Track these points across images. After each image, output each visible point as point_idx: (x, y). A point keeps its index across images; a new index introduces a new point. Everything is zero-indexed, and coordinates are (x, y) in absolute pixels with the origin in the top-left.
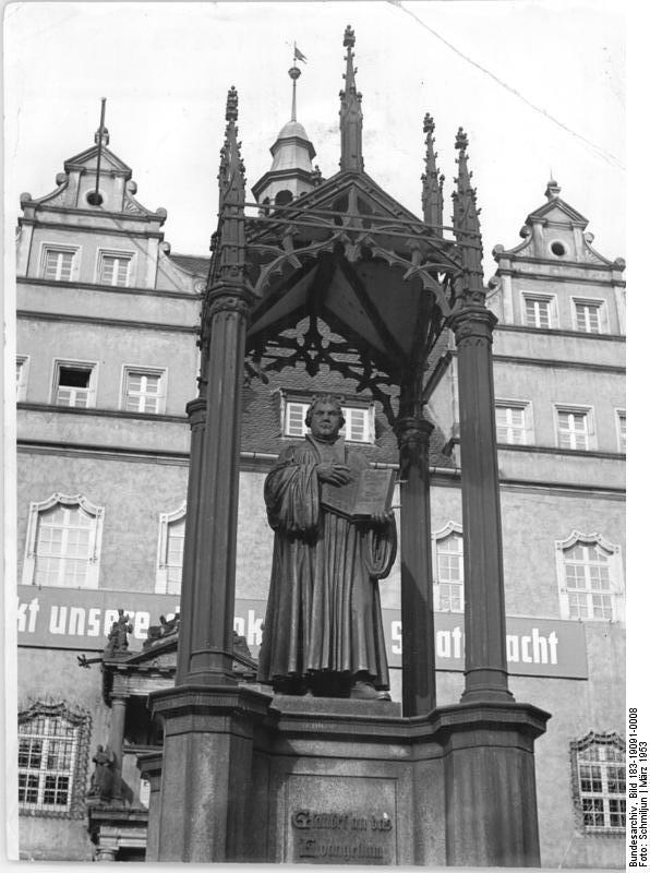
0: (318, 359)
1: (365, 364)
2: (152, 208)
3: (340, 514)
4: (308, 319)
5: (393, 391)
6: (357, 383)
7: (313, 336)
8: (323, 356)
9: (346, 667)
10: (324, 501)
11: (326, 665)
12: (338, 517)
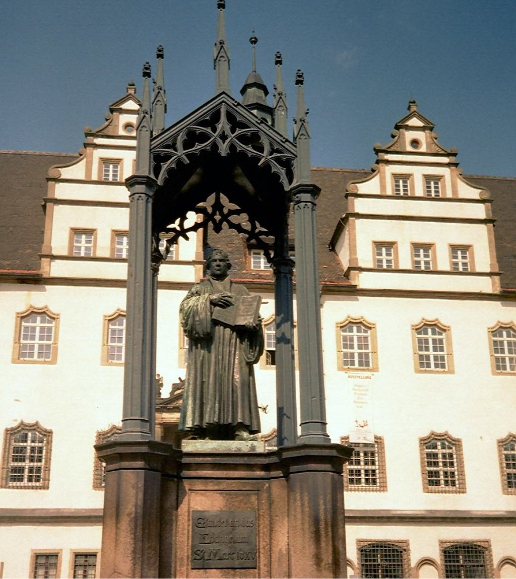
0: (221, 221)
1: (251, 221)
4: (214, 195)
6: (247, 236)
7: (218, 206)
8: (225, 218)
11: (216, 419)
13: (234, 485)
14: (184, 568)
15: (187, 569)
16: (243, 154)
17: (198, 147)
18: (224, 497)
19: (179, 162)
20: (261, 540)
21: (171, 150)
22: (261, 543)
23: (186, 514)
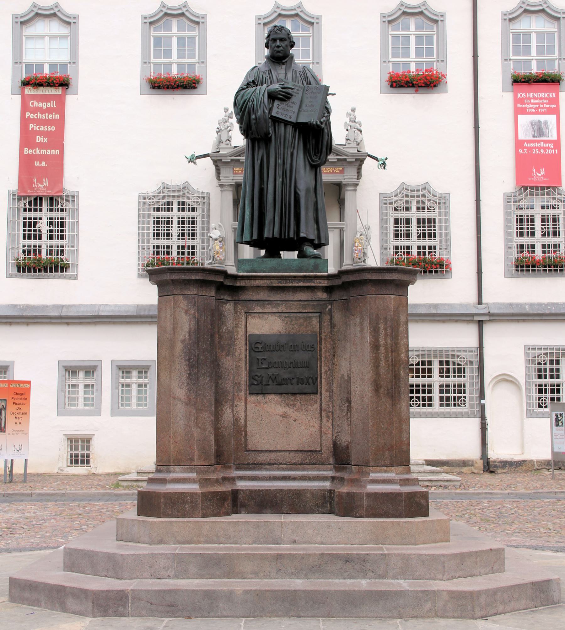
10: (274, 114)
11: (276, 235)
14: (242, 394)
15: (246, 394)
18: (283, 320)
20: (323, 365)
23: (243, 338)
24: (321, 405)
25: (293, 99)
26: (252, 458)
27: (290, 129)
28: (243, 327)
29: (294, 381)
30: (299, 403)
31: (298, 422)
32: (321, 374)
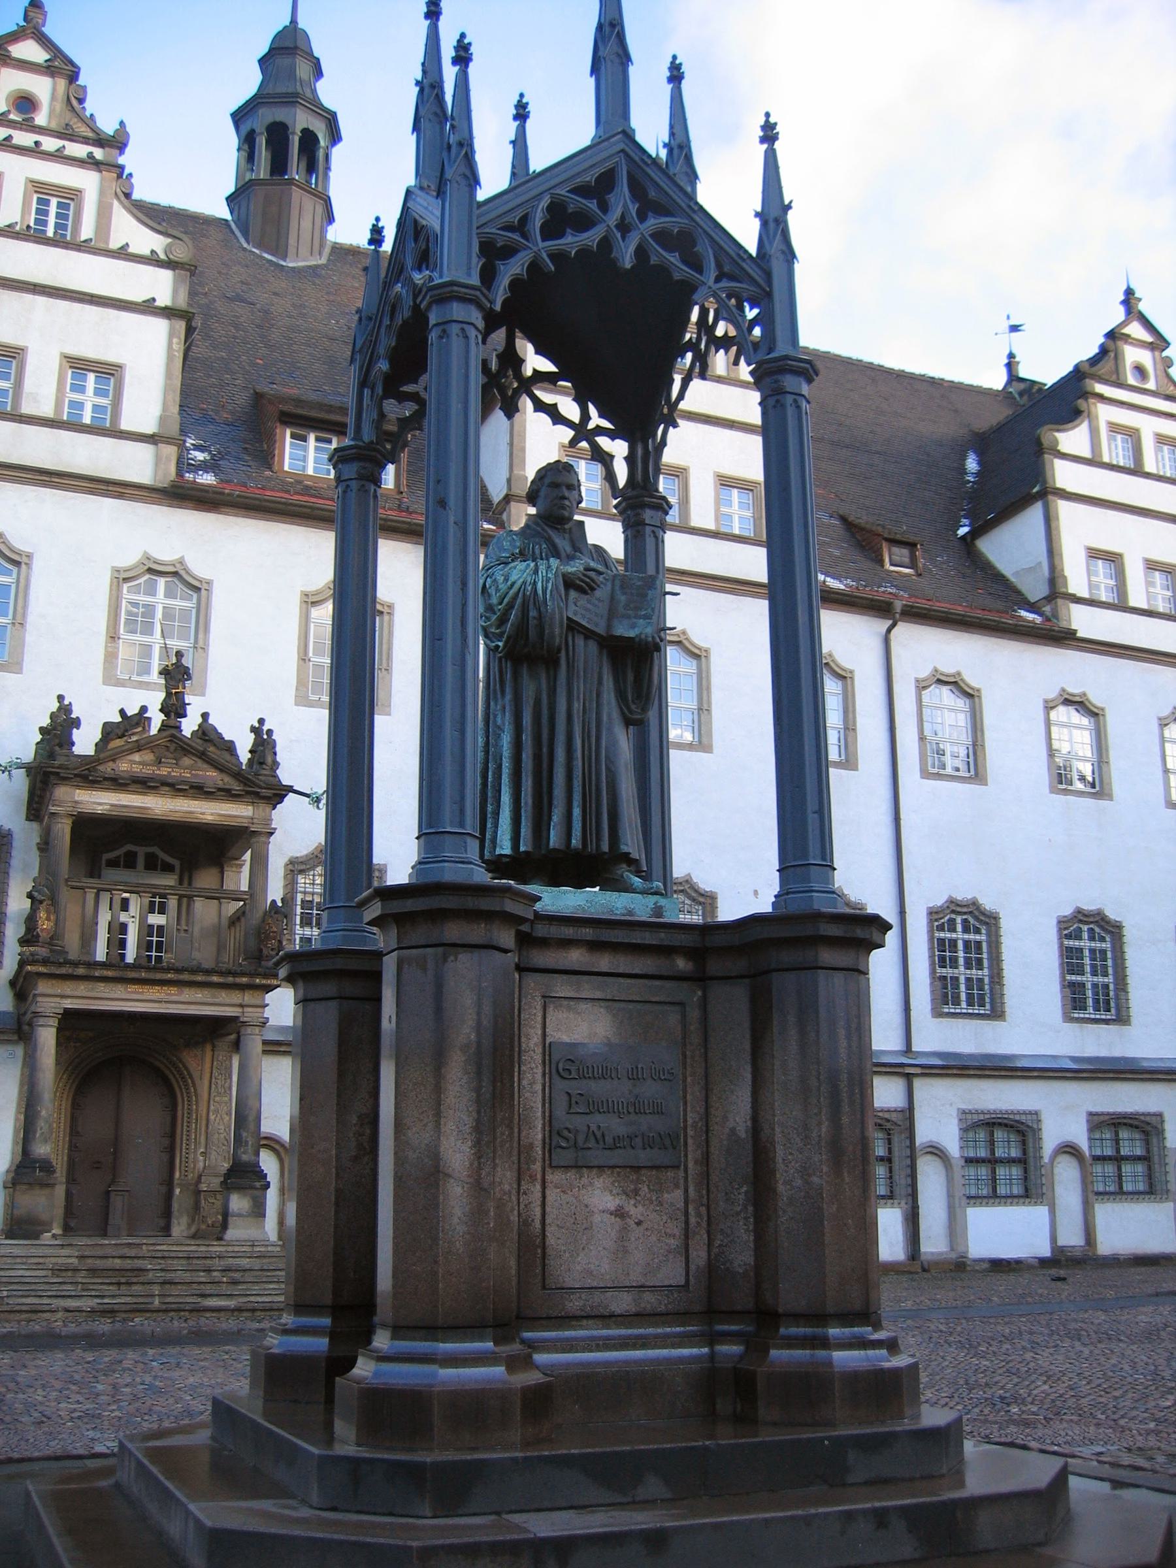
1: (581, 401)
2: (108, 126)
3: (588, 634)
5: (619, 448)
9: (605, 847)
12: (587, 638)
13: (635, 990)
16: (663, 270)
17: (571, 242)
19: (534, 267)
20: (689, 1109)
21: (516, 236)
22: (689, 1115)
23: (539, 1050)
24: (686, 1191)
25: (598, 593)
26: (574, 1304)
27: (593, 647)
28: (539, 1026)
29: (638, 1141)
30: (646, 1189)
31: (645, 1225)
32: (685, 1128)
